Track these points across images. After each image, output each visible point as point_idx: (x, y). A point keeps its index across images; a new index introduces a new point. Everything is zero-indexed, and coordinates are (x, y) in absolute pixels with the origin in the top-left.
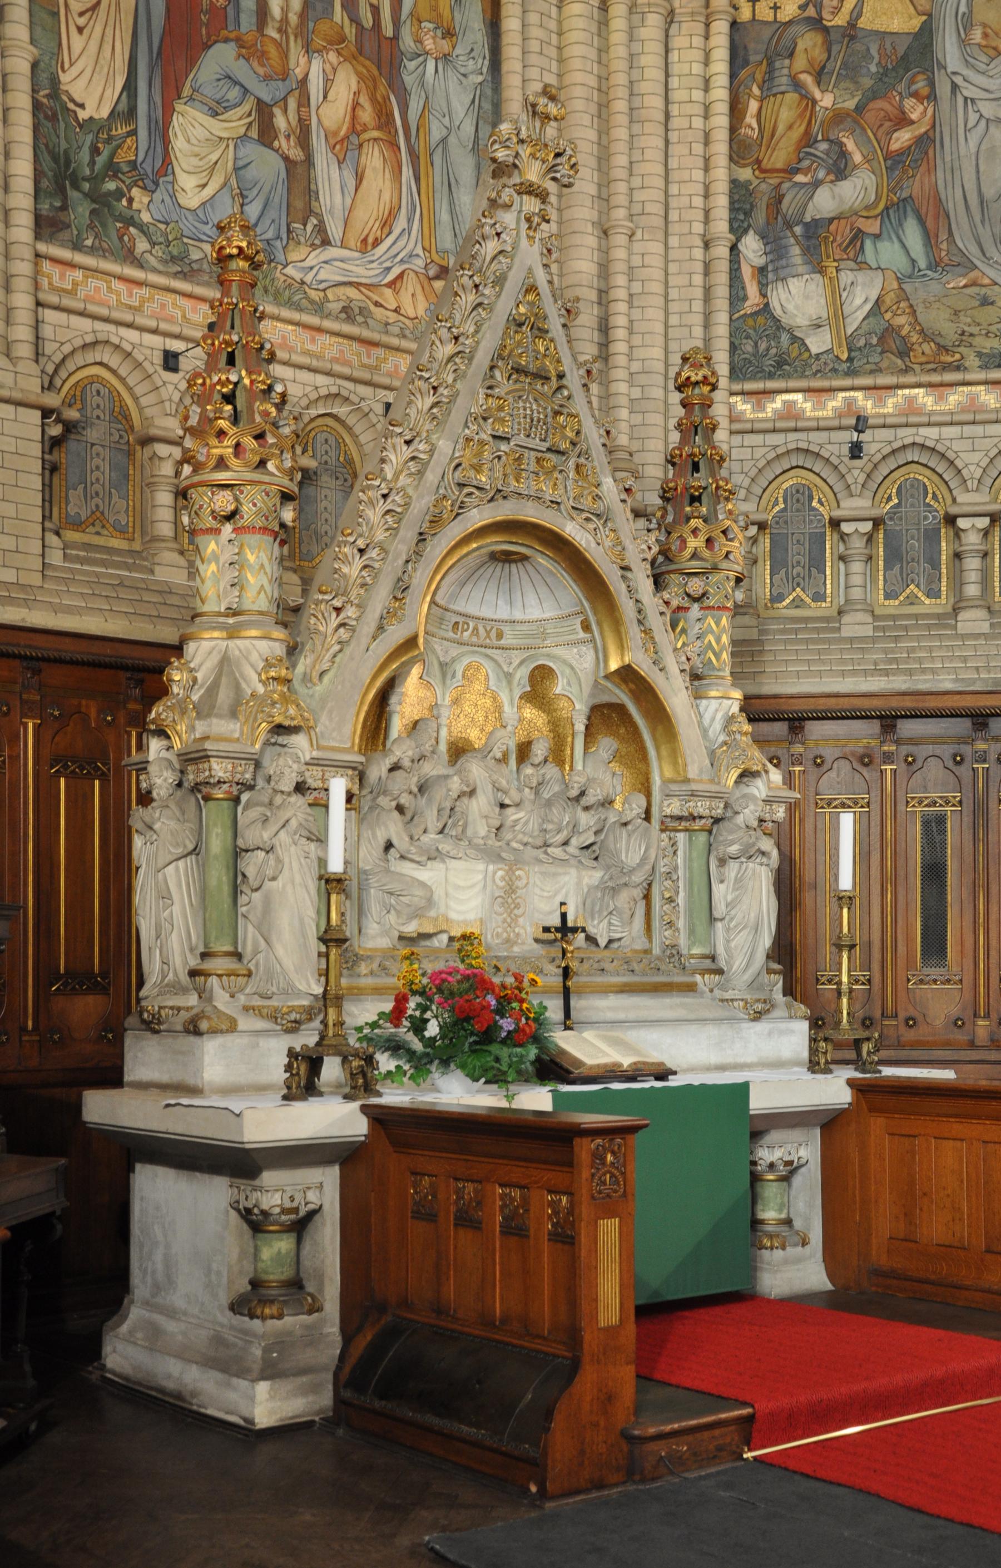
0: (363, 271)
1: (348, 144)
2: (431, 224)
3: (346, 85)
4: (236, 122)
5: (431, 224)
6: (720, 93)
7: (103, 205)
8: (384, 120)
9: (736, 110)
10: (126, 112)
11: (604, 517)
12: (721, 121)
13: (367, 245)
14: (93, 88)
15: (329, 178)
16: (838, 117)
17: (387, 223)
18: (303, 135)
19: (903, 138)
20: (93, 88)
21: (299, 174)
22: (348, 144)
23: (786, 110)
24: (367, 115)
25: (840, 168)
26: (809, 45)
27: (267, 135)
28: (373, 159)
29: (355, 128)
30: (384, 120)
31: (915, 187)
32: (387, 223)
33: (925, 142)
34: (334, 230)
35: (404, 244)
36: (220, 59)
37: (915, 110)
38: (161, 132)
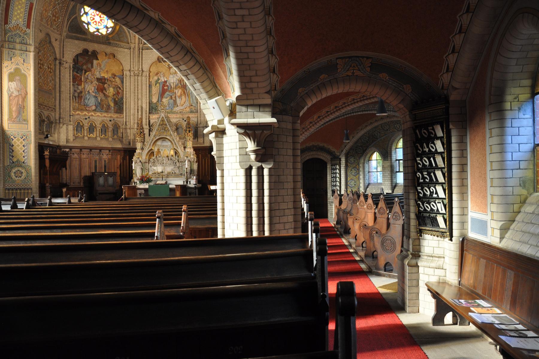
0: (182, 108)
1: (180, 97)
3: (180, 91)
4: (168, 98)
7: (156, 110)
10: (158, 101)
11: (171, 135)
14: (155, 100)
15: (178, 101)
17: (185, 103)
18: (175, 97)
20: (155, 100)
21: (175, 101)
24: (182, 93)
28: (183, 97)
29: (181, 94)
30: (184, 93)
32: (185, 103)
34: (179, 105)
35: (187, 104)
36: (167, 93)
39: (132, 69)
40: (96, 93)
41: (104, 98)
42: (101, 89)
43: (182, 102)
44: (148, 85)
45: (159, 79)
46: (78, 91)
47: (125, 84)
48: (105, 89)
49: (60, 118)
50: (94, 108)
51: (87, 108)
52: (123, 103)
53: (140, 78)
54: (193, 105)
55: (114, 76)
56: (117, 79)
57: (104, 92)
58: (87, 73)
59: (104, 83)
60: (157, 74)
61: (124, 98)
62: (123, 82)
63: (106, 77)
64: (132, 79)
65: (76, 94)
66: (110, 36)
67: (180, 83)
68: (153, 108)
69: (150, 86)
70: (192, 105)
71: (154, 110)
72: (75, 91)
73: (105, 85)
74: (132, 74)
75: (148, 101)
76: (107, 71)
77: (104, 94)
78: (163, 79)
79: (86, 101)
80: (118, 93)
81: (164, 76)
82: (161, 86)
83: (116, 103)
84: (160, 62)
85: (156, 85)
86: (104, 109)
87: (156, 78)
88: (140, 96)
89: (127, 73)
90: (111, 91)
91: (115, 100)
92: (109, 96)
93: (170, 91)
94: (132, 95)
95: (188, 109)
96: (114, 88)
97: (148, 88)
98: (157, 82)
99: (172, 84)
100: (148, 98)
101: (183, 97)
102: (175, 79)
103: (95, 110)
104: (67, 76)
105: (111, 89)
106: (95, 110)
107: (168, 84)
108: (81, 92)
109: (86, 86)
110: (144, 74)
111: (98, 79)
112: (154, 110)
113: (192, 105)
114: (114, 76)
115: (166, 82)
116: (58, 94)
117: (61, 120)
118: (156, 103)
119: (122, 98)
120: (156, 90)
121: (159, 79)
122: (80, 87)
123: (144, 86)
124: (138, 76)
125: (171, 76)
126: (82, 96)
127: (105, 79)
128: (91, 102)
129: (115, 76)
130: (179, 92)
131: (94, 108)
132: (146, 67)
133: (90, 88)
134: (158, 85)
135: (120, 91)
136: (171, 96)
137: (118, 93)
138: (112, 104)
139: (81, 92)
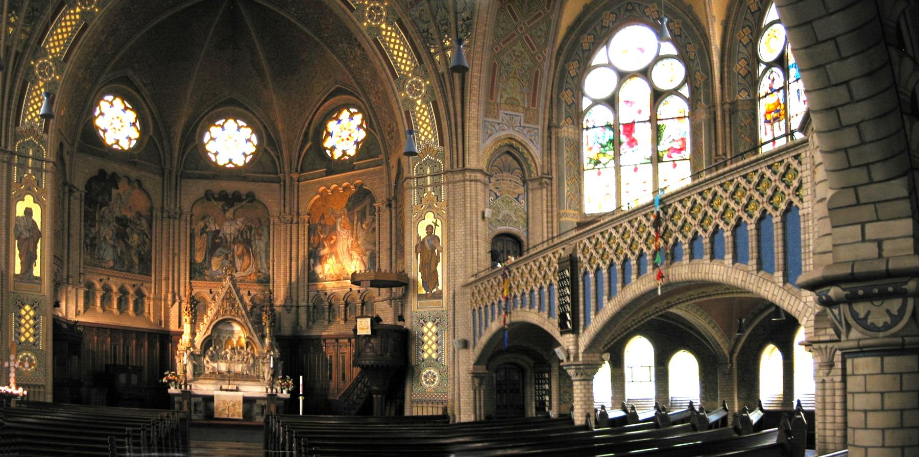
0: (243, 274)
2: (256, 264)
4: (222, 257)
5: (256, 264)
6: (306, 237)
8: (248, 251)
9: (309, 239)
10: (205, 260)
12: (306, 241)
13: (244, 271)
15: (238, 263)
16: (324, 239)
18: (233, 257)
19: (332, 242)
20: (199, 259)
21: (233, 263)
22: (241, 257)
23: (316, 239)
25: (324, 247)
26: (319, 227)
27: (227, 258)
28: (246, 258)
30: (248, 251)
31: (334, 250)
32: (248, 266)
33: (335, 242)
35: (252, 269)
36: (220, 249)
37: (334, 237)
38: (210, 262)
39: (166, 208)
40: (114, 241)
41: (124, 250)
42: (121, 236)
43: (245, 266)
44: (188, 234)
45: (206, 227)
46: (91, 236)
47: (154, 230)
48: (127, 236)
49: (68, 276)
50: (111, 264)
51: (103, 264)
52: (150, 260)
53: (177, 222)
54: (263, 271)
55: (139, 215)
56: (144, 221)
57: (126, 240)
58: (104, 209)
59: (126, 226)
60: (203, 218)
61: (153, 251)
62: (150, 226)
63: (129, 216)
64: (164, 223)
65: (88, 241)
66: (136, 153)
67: (242, 235)
68: (196, 271)
69: (192, 237)
70: (259, 272)
71: (197, 274)
72: (86, 235)
73: (128, 230)
74: (165, 215)
75: (188, 260)
76: (130, 207)
77: (126, 243)
78: (213, 227)
79: (101, 253)
80: (144, 243)
81: (215, 222)
82: (210, 237)
83: (141, 260)
84: (209, 200)
85: (201, 234)
86: (126, 267)
87: (202, 224)
88: (176, 251)
89: (157, 213)
90: (135, 239)
91: (140, 254)
92: (132, 247)
93: (224, 247)
94: (164, 248)
95: (253, 277)
96: (138, 234)
97: (188, 238)
98: (203, 231)
99: (228, 236)
100: (188, 255)
101: (246, 258)
102: (233, 229)
103: (113, 268)
104: (77, 211)
105: (136, 237)
106: (113, 268)
107: (220, 235)
108: (95, 238)
109: (102, 228)
110: (183, 217)
111: (118, 220)
112: (197, 274)
113: (259, 272)
114: (139, 215)
115: (218, 232)
116: (66, 239)
117: (71, 280)
118: (201, 264)
119: (150, 251)
120: (200, 242)
121: (206, 227)
122: (93, 230)
123: (183, 235)
124: (175, 218)
125: (227, 223)
126: (95, 245)
127: (127, 220)
128: (109, 255)
129: (141, 216)
130: (238, 249)
131: (111, 264)
132: (186, 205)
133: (107, 232)
134: (204, 235)
135: (147, 240)
136: (227, 255)
137: (144, 243)
138: (136, 261)
139: (95, 238)
